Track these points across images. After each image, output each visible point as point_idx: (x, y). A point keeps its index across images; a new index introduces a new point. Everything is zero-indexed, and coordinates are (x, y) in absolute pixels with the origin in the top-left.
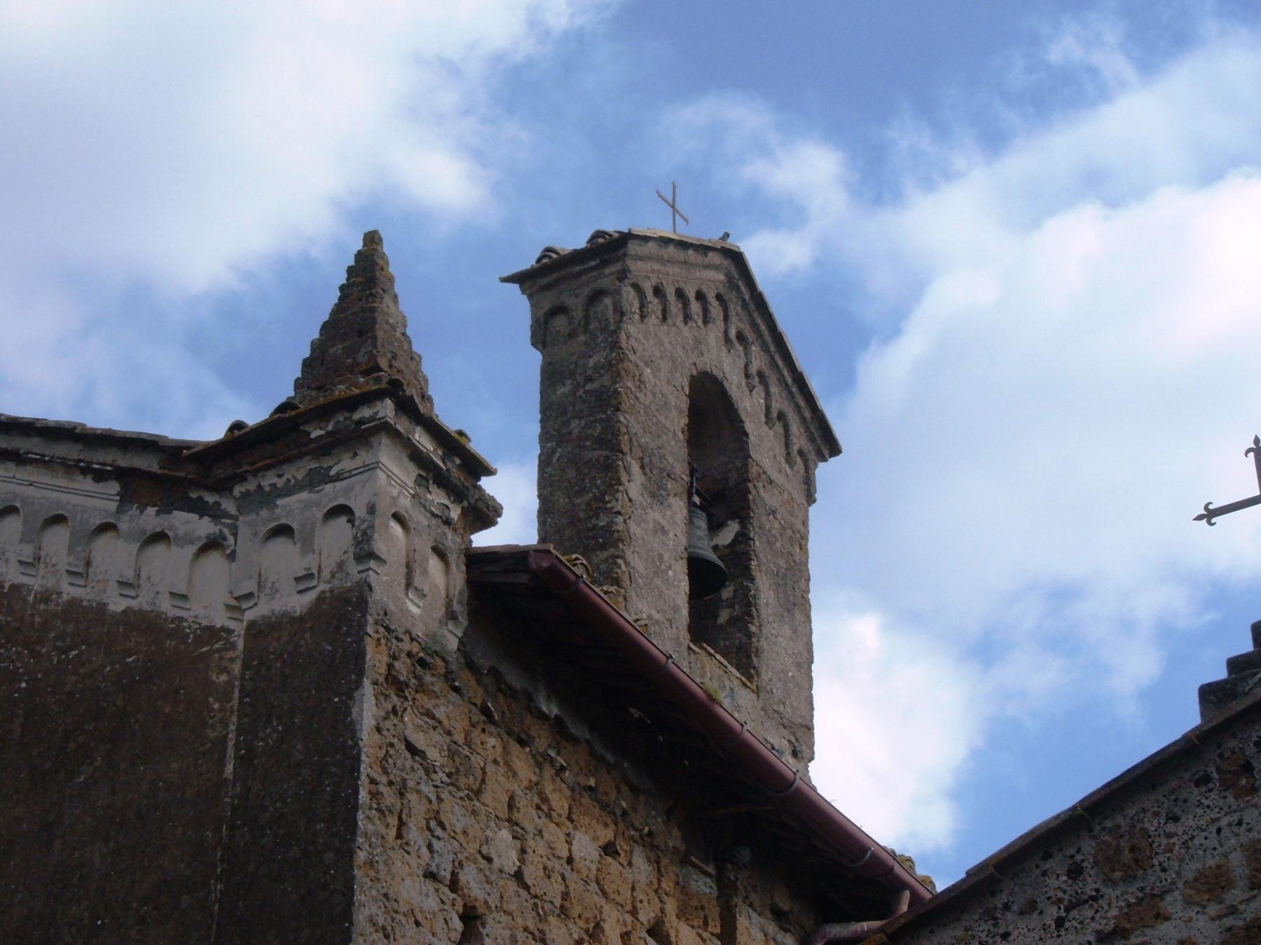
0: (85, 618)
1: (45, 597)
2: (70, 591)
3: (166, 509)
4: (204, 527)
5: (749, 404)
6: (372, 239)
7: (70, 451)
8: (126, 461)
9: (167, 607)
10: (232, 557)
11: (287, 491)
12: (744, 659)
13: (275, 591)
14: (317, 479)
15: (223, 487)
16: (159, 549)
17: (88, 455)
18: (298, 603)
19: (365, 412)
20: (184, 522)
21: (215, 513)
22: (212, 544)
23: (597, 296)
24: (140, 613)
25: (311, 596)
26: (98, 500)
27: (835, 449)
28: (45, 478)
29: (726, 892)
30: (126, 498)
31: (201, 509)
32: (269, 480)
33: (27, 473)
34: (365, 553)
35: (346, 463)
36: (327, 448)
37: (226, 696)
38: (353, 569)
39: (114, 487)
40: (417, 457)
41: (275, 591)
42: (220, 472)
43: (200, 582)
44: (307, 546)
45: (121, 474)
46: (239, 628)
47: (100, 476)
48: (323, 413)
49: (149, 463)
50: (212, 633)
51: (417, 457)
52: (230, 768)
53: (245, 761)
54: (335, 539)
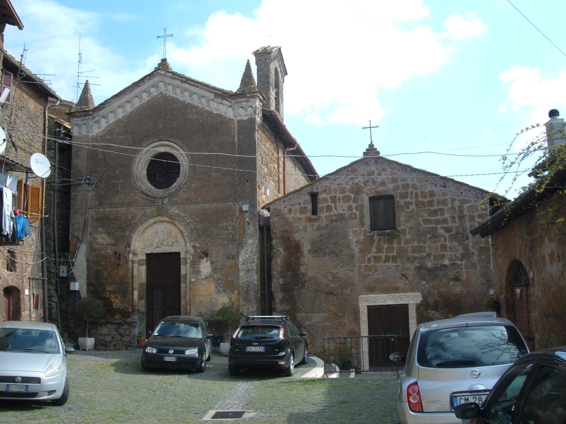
0: (210, 113)
1: (202, 108)
2: (207, 108)
3: (222, 99)
4: (229, 104)
5: (279, 70)
6: (248, 61)
7: (207, 88)
8: (216, 92)
9: (223, 114)
10: (234, 109)
11: (243, 102)
12: (279, 112)
13: (241, 116)
14: (247, 101)
15: (233, 99)
16: (221, 105)
17: (209, 89)
18: (245, 118)
19: (255, 94)
20: (224, 102)
21: (230, 102)
22: (230, 106)
23: (266, 59)
24: (219, 114)
25: (247, 118)
26: (212, 96)
27: (287, 74)
28: (201, 90)
29: (277, 146)
30: (215, 96)
31: (228, 101)
32: (240, 100)
33: (198, 89)
34: (255, 113)
35: (252, 100)
36: (249, 97)
37: (234, 129)
38: (253, 116)
39: (213, 94)
40: (260, 99)
41: (241, 116)
42: (233, 97)
43: (226, 110)
44: (246, 111)
45: (215, 93)
46: (236, 121)
47: (211, 92)
48: (249, 93)
49: (221, 93)
50: (230, 119)
51: (260, 99)
52: (236, 139)
53: (239, 139)
54: (250, 110)
